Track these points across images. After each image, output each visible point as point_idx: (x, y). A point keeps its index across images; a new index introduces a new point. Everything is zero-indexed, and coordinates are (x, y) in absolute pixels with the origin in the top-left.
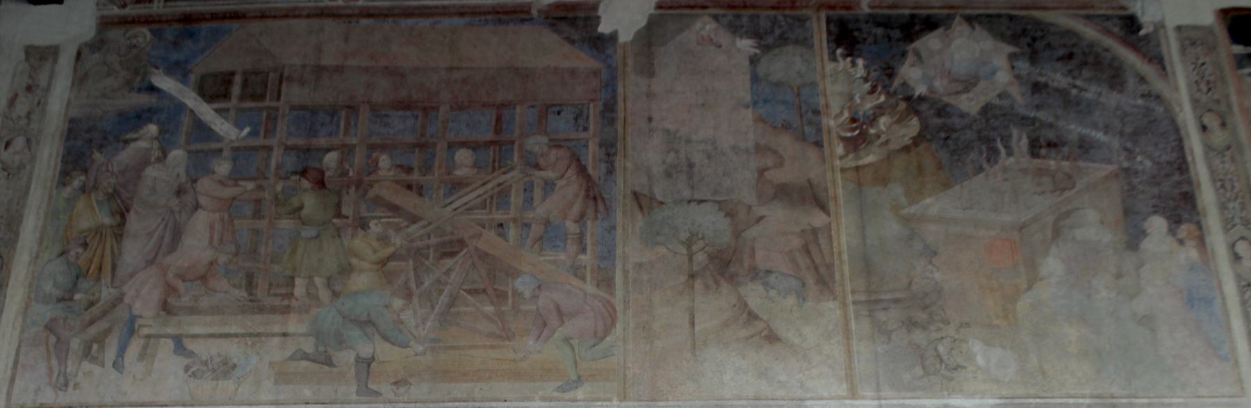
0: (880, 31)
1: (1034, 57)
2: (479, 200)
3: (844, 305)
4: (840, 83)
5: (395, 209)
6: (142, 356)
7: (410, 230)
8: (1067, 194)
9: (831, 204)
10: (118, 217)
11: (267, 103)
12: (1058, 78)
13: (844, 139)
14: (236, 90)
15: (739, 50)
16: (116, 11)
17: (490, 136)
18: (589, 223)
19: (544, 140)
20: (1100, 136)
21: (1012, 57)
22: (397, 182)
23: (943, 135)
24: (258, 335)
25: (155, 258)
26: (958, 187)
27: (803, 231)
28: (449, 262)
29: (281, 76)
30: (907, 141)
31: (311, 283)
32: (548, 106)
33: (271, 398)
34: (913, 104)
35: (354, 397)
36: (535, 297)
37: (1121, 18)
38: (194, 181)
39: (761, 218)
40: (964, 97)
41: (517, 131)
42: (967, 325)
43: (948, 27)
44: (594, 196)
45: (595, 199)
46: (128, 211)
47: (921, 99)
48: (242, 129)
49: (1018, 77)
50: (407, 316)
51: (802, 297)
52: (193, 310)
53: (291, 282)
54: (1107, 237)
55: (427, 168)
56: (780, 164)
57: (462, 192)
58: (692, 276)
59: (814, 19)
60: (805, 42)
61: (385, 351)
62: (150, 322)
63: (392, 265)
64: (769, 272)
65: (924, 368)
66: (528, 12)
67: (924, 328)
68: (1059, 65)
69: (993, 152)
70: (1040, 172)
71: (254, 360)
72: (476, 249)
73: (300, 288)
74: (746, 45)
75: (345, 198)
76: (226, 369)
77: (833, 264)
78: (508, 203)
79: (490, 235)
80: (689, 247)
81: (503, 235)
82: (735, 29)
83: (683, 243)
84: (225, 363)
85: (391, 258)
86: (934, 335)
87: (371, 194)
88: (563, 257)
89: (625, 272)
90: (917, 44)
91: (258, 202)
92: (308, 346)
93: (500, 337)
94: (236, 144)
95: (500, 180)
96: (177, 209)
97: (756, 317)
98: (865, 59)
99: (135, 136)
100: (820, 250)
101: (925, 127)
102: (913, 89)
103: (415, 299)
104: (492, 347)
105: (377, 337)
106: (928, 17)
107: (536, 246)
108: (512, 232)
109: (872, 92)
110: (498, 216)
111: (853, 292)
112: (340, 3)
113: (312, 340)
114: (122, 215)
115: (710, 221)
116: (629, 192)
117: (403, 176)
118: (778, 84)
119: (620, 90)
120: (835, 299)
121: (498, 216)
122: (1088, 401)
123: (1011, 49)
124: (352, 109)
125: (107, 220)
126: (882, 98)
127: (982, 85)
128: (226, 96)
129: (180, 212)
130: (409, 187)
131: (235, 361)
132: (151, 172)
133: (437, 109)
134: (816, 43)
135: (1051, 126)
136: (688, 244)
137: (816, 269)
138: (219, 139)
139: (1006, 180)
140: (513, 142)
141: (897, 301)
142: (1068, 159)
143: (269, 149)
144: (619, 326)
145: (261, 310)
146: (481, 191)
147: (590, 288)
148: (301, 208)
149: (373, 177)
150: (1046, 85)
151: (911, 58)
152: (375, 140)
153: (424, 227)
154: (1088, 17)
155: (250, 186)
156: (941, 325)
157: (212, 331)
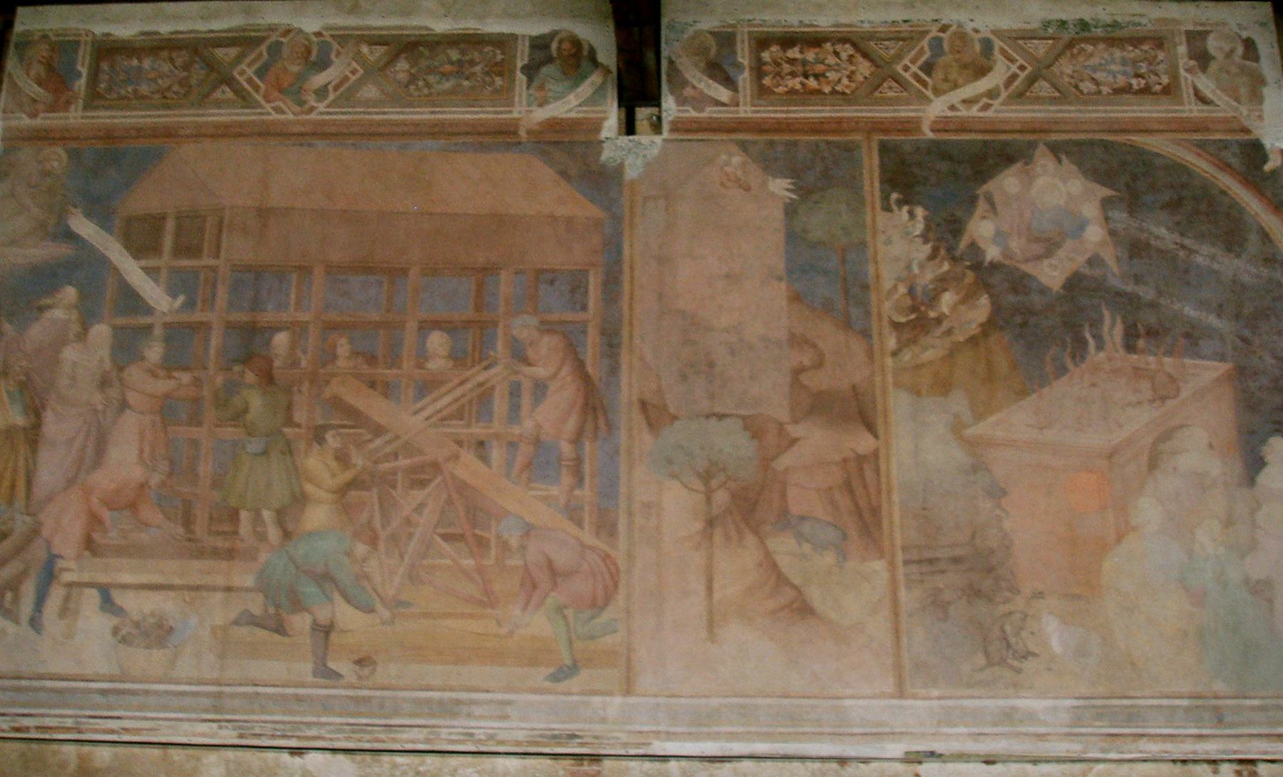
0: (944, 166)
1: (1133, 203)
2: (455, 406)
3: (892, 565)
4: (898, 243)
5: (354, 415)
6: (64, 611)
7: (372, 446)
8: (1170, 404)
9: (880, 421)
10: (33, 417)
11: (206, 261)
12: (1161, 232)
13: (896, 326)
14: (168, 242)
15: (773, 195)
16: (26, 121)
17: (469, 313)
18: (587, 446)
19: (533, 321)
20: (1212, 320)
21: (1106, 203)
22: (358, 376)
23: (1018, 319)
24: (198, 588)
25: (76, 476)
26: (1034, 396)
27: (845, 460)
28: (418, 495)
29: (221, 223)
30: (974, 329)
31: (257, 519)
32: (539, 272)
33: (215, 675)
34: (983, 274)
35: (310, 679)
36: (523, 547)
37: (1241, 144)
38: (121, 369)
39: (794, 441)
40: (1046, 262)
41: (502, 309)
42: (1039, 595)
43: (1028, 159)
44: (594, 406)
45: (594, 409)
46: (44, 407)
47: (994, 266)
48: (174, 296)
49: (1112, 233)
50: (373, 566)
51: (843, 555)
52: (120, 551)
53: (234, 516)
54: (1215, 467)
55: (394, 359)
56: (819, 364)
57: (436, 394)
58: (711, 523)
59: (864, 150)
60: (853, 184)
61: (346, 615)
62: (72, 564)
63: (354, 495)
64: (802, 518)
65: (987, 654)
66: (515, 133)
67: (990, 600)
68: (1163, 216)
69: (1081, 343)
70: (1138, 372)
71: (194, 621)
72: (452, 474)
73: (245, 527)
74: (780, 187)
75: (296, 397)
76: (158, 633)
77: (880, 507)
78: (490, 414)
79: (468, 456)
80: (706, 483)
81: (485, 459)
82: (769, 165)
83: (699, 475)
84: (160, 626)
85: (353, 484)
86: (1002, 609)
87: (328, 392)
88: (555, 491)
89: (630, 514)
90: (990, 186)
91: (197, 401)
92: (256, 605)
93: (481, 603)
94: (168, 319)
95: (480, 378)
96: (100, 408)
97: (787, 582)
98: (926, 207)
99: (49, 301)
100: (865, 487)
101: (997, 309)
102: (984, 252)
103: (382, 546)
104: (471, 616)
105: (337, 597)
106: (1006, 144)
107: (525, 476)
108: (496, 454)
109: (932, 257)
110: (478, 430)
111: (904, 548)
112: (291, 117)
113: (260, 598)
114: (36, 412)
115: (732, 444)
116: (635, 398)
117: (365, 369)
118: (816, 245)
119: (626, 251)
120: (882, 557)
121: (478, 430)
122: (1185, 702)
123: (1106, 192)
124: (305, 270)
125: (20, 420)
126: (946, 267)
127: (1069, 244)
128: (156, 250)
129: (104, 411)
130: (372, 385)
131: (171, 623)
132: (70, 354)
133: (404, 272)
134: (866, 182)
135: (1153, 305)
136: (706, 477)
137: (861, 516)
138: (149, 311)
139: (1094, 385)
140: (495, 324)
141: (956, 560)
142: (1169, 353)
143: (205, 327)
144: (622, 591)
145: (201, 554)
146: (458, 392)
147: (588, 538)
148: (246, 411)
149: (329, 368)
150: (1148, 245)
151: (982, 206)
152: (333, 316)
153: (389, 442)
154: (1201, 145)
155: (186, 378)
156: (1008, 594)
157: (143, 579)
